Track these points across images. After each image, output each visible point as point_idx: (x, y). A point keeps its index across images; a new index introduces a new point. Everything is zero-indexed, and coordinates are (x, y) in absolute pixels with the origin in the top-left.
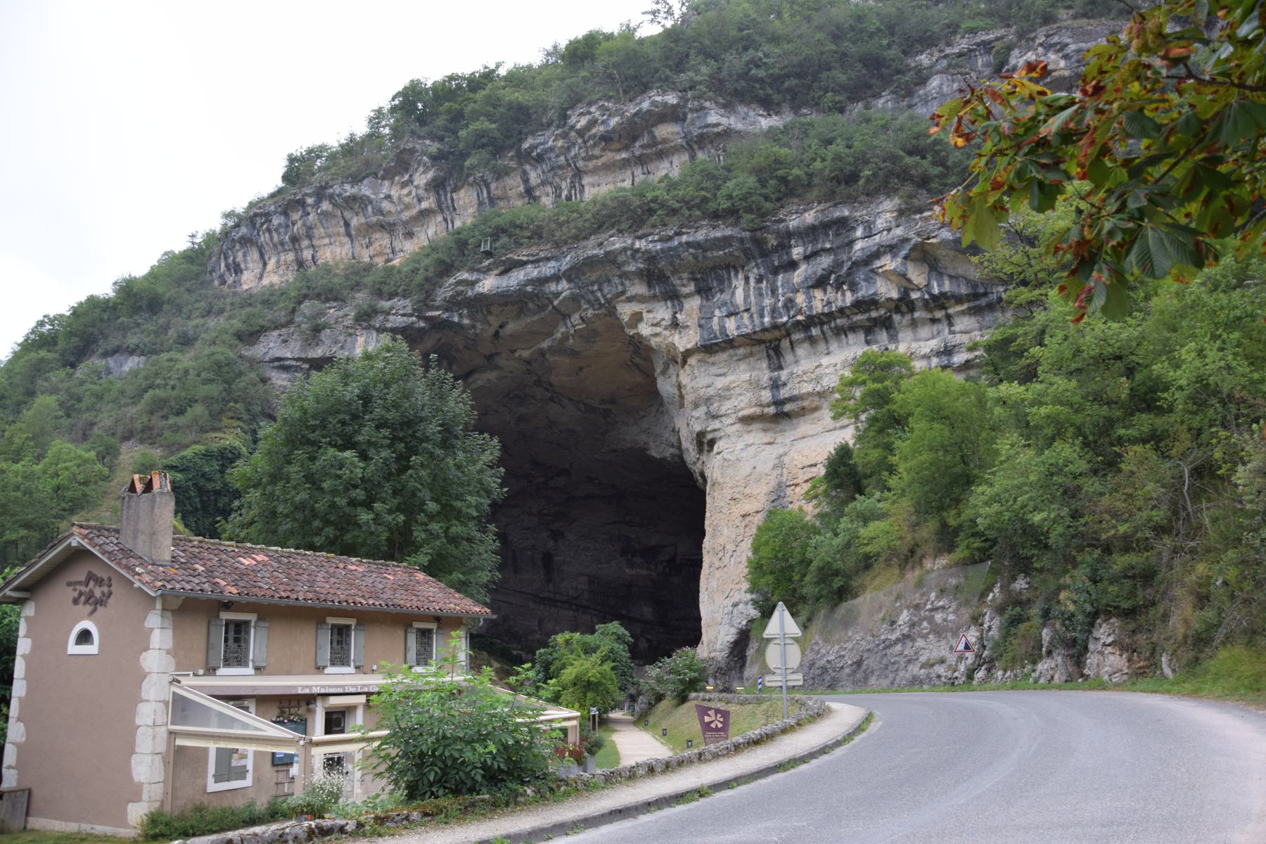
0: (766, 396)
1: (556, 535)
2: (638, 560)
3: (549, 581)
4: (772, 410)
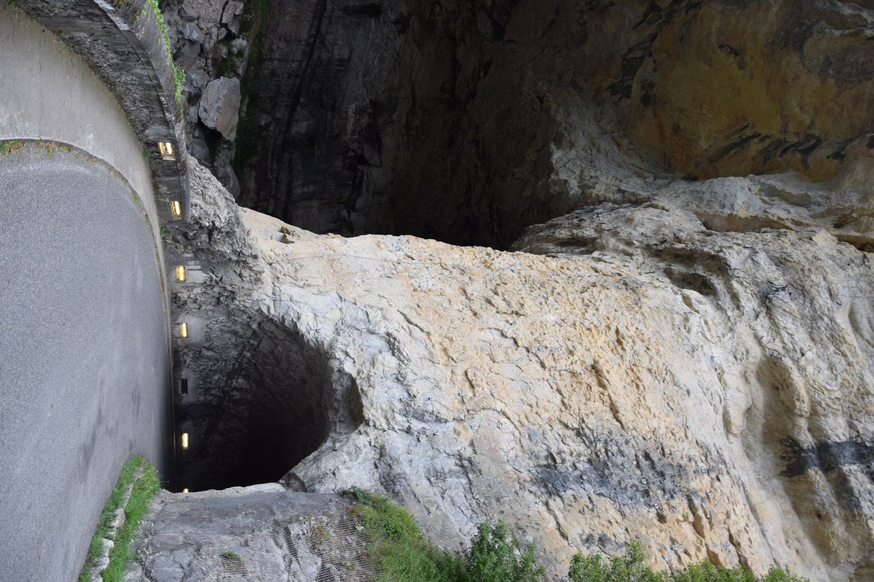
0: (837, 430)
1: (402, 24)
2: (365, 120)
3: (346, 11)
4: (806, 440)
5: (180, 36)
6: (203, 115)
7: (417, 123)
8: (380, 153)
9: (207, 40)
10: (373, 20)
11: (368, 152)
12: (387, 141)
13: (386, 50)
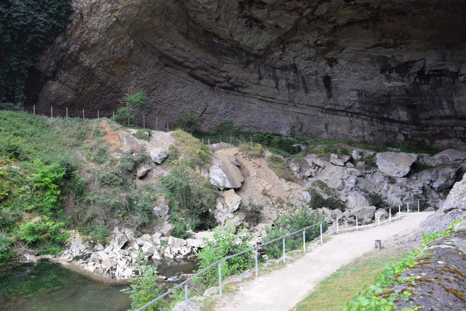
1: (332, 62)
2: (394, 75)
5: (354, 189)
6: (402, 174)
7: (392, 41)
8: (415, 61)
9: (355, 173)
10: (332, 80)
11: (415, 69)
12: (406, 58)
13: (349, 69)
